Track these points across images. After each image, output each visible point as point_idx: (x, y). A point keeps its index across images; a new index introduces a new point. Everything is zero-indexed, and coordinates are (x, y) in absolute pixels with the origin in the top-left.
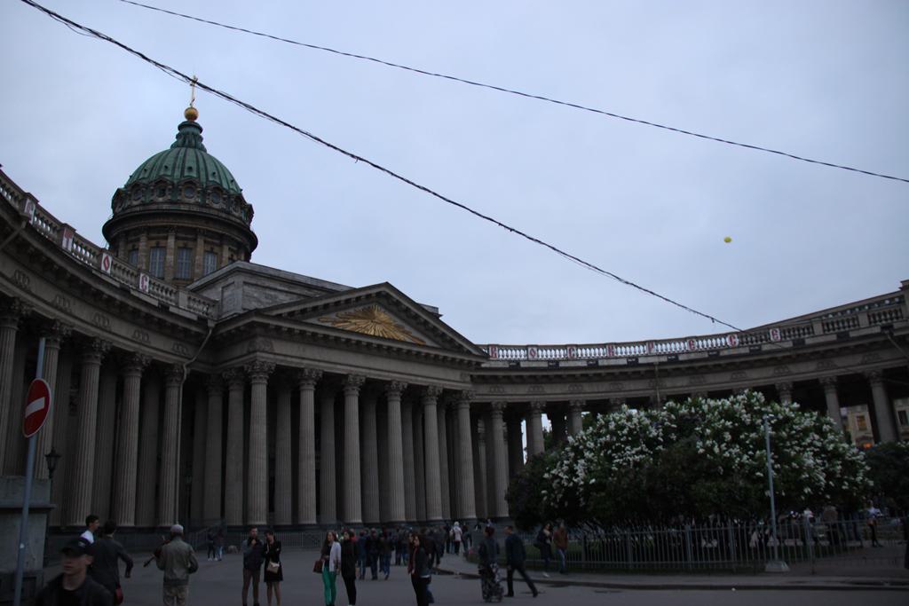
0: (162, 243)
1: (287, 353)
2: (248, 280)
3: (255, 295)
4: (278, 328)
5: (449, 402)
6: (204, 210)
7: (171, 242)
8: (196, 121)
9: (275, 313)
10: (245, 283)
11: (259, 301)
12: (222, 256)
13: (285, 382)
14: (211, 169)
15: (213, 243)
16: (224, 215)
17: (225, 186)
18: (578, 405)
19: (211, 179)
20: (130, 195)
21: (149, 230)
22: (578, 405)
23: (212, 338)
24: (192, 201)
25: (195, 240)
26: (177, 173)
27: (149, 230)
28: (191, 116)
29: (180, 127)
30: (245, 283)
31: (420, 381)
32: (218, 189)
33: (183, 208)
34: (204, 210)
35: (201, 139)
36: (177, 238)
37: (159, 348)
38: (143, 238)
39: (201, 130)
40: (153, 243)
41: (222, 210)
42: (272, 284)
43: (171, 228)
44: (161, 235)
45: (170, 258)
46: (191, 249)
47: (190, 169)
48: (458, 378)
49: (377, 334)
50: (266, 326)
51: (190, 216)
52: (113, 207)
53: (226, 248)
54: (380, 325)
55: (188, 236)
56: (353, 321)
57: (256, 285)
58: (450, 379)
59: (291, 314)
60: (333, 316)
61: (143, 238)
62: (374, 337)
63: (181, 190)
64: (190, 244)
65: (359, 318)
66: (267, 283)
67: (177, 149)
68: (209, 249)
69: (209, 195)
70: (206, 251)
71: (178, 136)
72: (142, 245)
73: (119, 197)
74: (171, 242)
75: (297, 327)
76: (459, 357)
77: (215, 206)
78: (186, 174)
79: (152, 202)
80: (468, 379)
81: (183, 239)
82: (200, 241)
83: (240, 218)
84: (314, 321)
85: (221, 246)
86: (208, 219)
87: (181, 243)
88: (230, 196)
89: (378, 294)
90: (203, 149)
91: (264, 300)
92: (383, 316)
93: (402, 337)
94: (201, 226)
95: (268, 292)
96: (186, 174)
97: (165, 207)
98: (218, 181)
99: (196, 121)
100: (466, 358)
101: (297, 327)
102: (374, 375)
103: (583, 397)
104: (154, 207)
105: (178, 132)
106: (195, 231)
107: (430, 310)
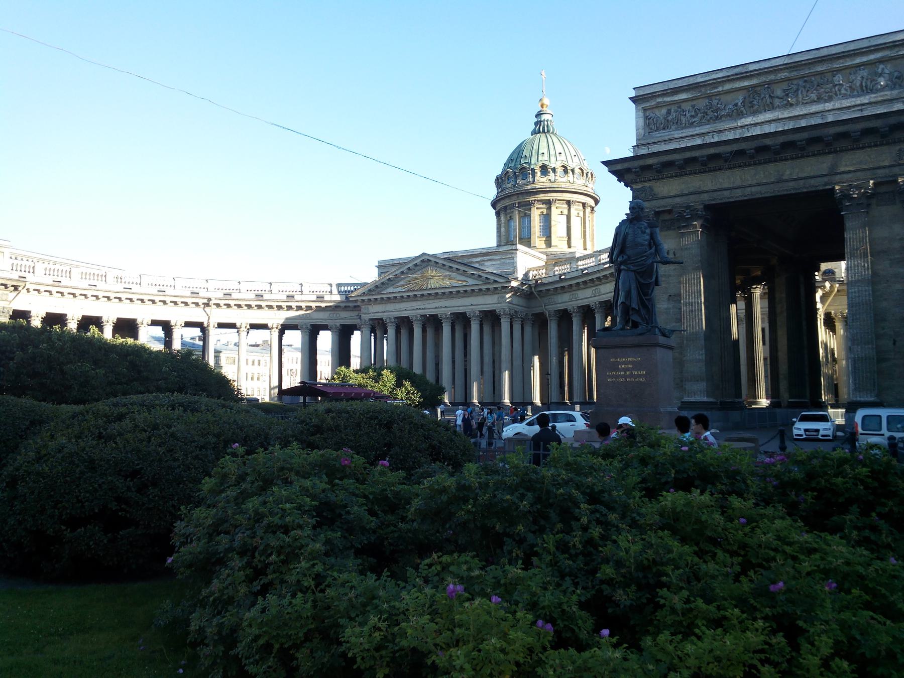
5: (491, 318)
17: (533, 161)
24: (510, 185)
31: (461, 310)
36: (506, 215)
48: (495, 301)
49: (429, 287)
51: (509, 196)
54: (437, 280)
58: (488, 302)
59: (370, 290)
60: (402, 283)
63: (505, 181)
68: (522, 215)
69: (518, 176)
70: (520, 217)
71: (536, 124)
81: (510, 213)
84: (390, 290)
89: (423, 261)
93: (447, 283)
100: (491, 287)
101: (372, 297)
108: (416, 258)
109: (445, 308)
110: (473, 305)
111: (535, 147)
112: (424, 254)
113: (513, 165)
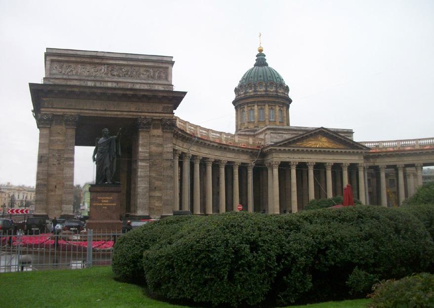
0: (253, 108)
1: (285, 157)
2: (272, 132)
3: (275, 136)
4: (280, 150)
6: (267, 93)
7: (256, 107)
8: (262, 52)
9: (278, 145)
10: (271, 133)
11: (276, 138)
12: (276, 110)
13: (284, 168)
14: (269, 74)
15: (272, 105)
16: (275, 93)
17: (275, 81)
18: (419, 165)
19: (269, 79)
20: (240, 90)
21: (247, 103)
22: (419, 165)
23: (261, 153)
24: (262, 90)
25: (265, 105)
26: (256, 79)
27: (247, 103)
28: (261, 51)
29: (257, 56)
30: (271, 133)
31: (339, 162)
32: (272, 84)
33: (259, 93)
34: (267, 93)
35: (266, 60)
36: (258, 105)
37: (243, 159)
38: (246, 107)
39: (265, 56)
40: (249, 108)
41: (273, 92)
42: (281, 132)
43: (254, 102)
44: (252, 105)
45: (256, 114)
46: (263, 109)
47: (260, 76)
50: (275, 149)
51: (262, 96)
52: (236, 93)
53: (277, 106)
54: (323, 142)
55: (262, 104)
56: (310, 142)
57: (275, 133)
59: (285, 144)
61: (246, 107)
62: (319, 148)
64: (263, 107)
65: (312, 141)
66: (279, 132)
67: (256, 67)
68: (270, 107)
70: (269, 109)
71: (256, 60)
72: (246, 109)
73: (236, 90)
74: (256, 107)
75: (287, 149)
76: (356, 151)
77: (272, 90)
78: (259, 79)
79: (247, 92)
80: (362, 158)
81: (260, 105)
82: (267, 106)
83: (282, 93)
85: (275, 106)
86: (269, 96)
87: (260, 107)
88: (276, 85)
90: (267, 65)
91: (278, 137)
92: (324, 139)
93: (330, 146)
94: (265, 99)
95: (280, 135)
96: (259, 79)
97: (252, 94)
98: (271, 79)
99: (262, 52)
102: (319, 161)
103: (422, 162)
104: (248, 94)
105: (256, 58)
106: (264, 102)
107: (350, 131)
108: (319, 129)
109: (330, 160)
110: (346, 160)
111: (273, 75)
112: (322, 128)
113: (262, 79)
